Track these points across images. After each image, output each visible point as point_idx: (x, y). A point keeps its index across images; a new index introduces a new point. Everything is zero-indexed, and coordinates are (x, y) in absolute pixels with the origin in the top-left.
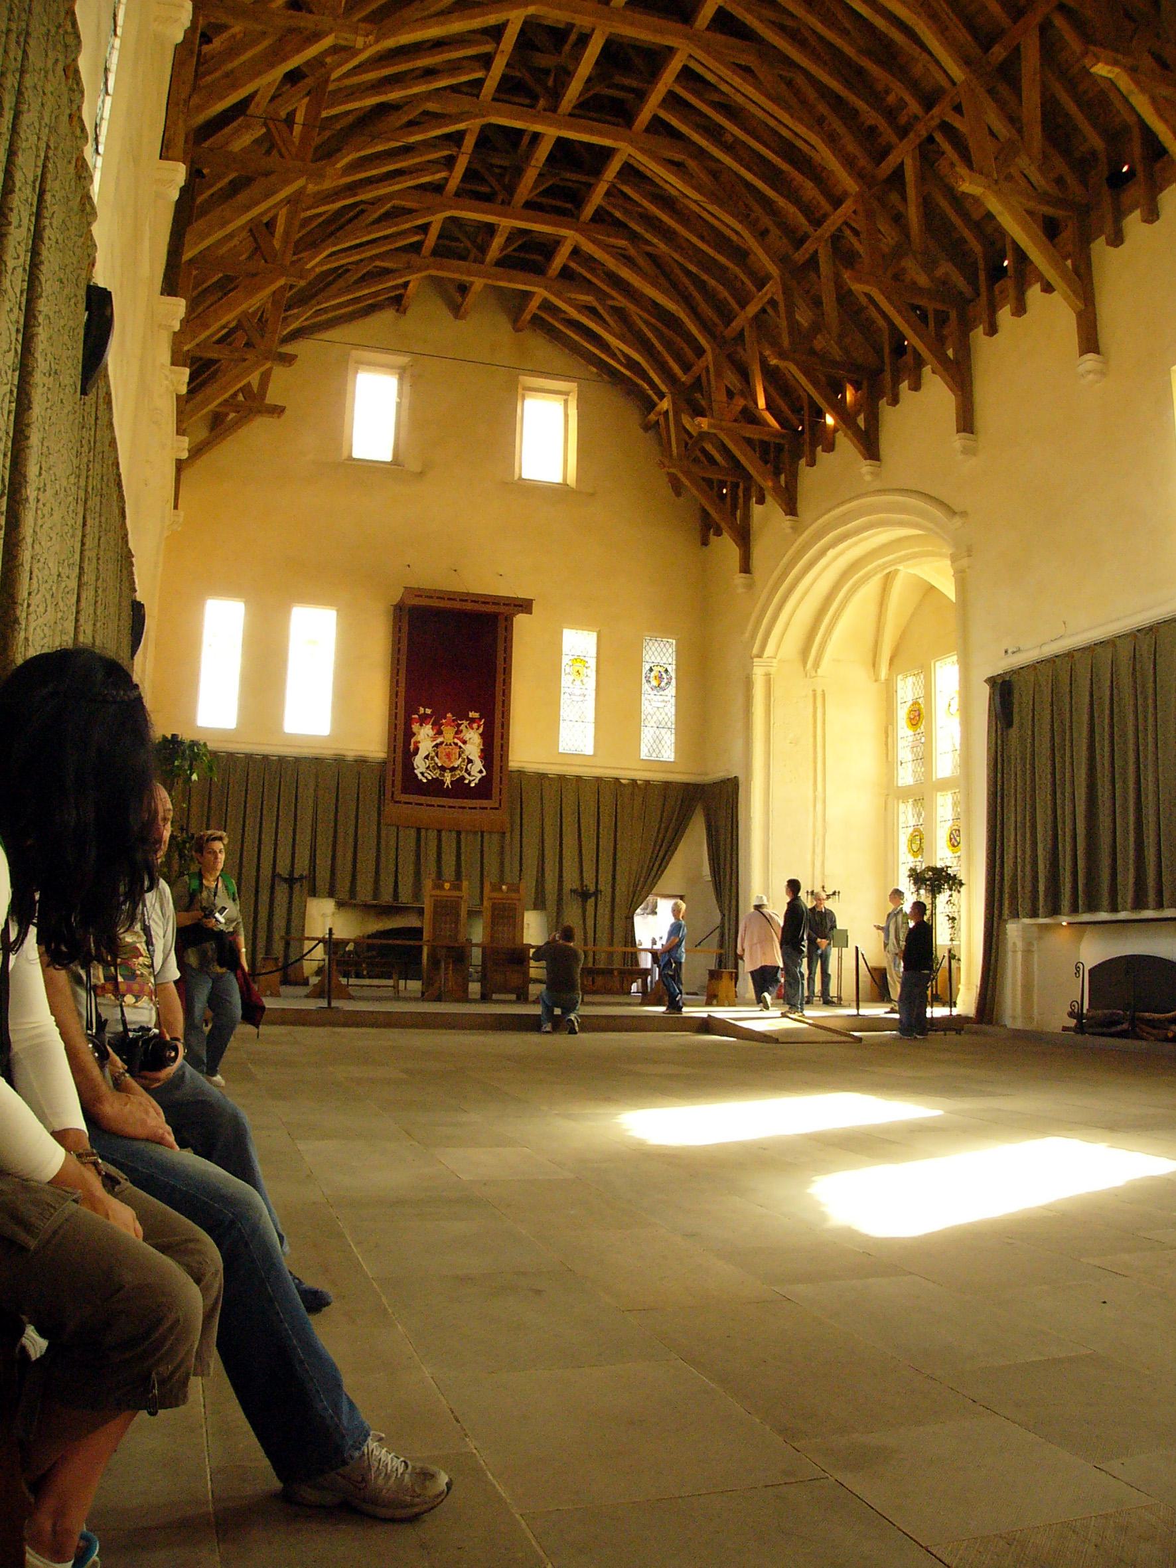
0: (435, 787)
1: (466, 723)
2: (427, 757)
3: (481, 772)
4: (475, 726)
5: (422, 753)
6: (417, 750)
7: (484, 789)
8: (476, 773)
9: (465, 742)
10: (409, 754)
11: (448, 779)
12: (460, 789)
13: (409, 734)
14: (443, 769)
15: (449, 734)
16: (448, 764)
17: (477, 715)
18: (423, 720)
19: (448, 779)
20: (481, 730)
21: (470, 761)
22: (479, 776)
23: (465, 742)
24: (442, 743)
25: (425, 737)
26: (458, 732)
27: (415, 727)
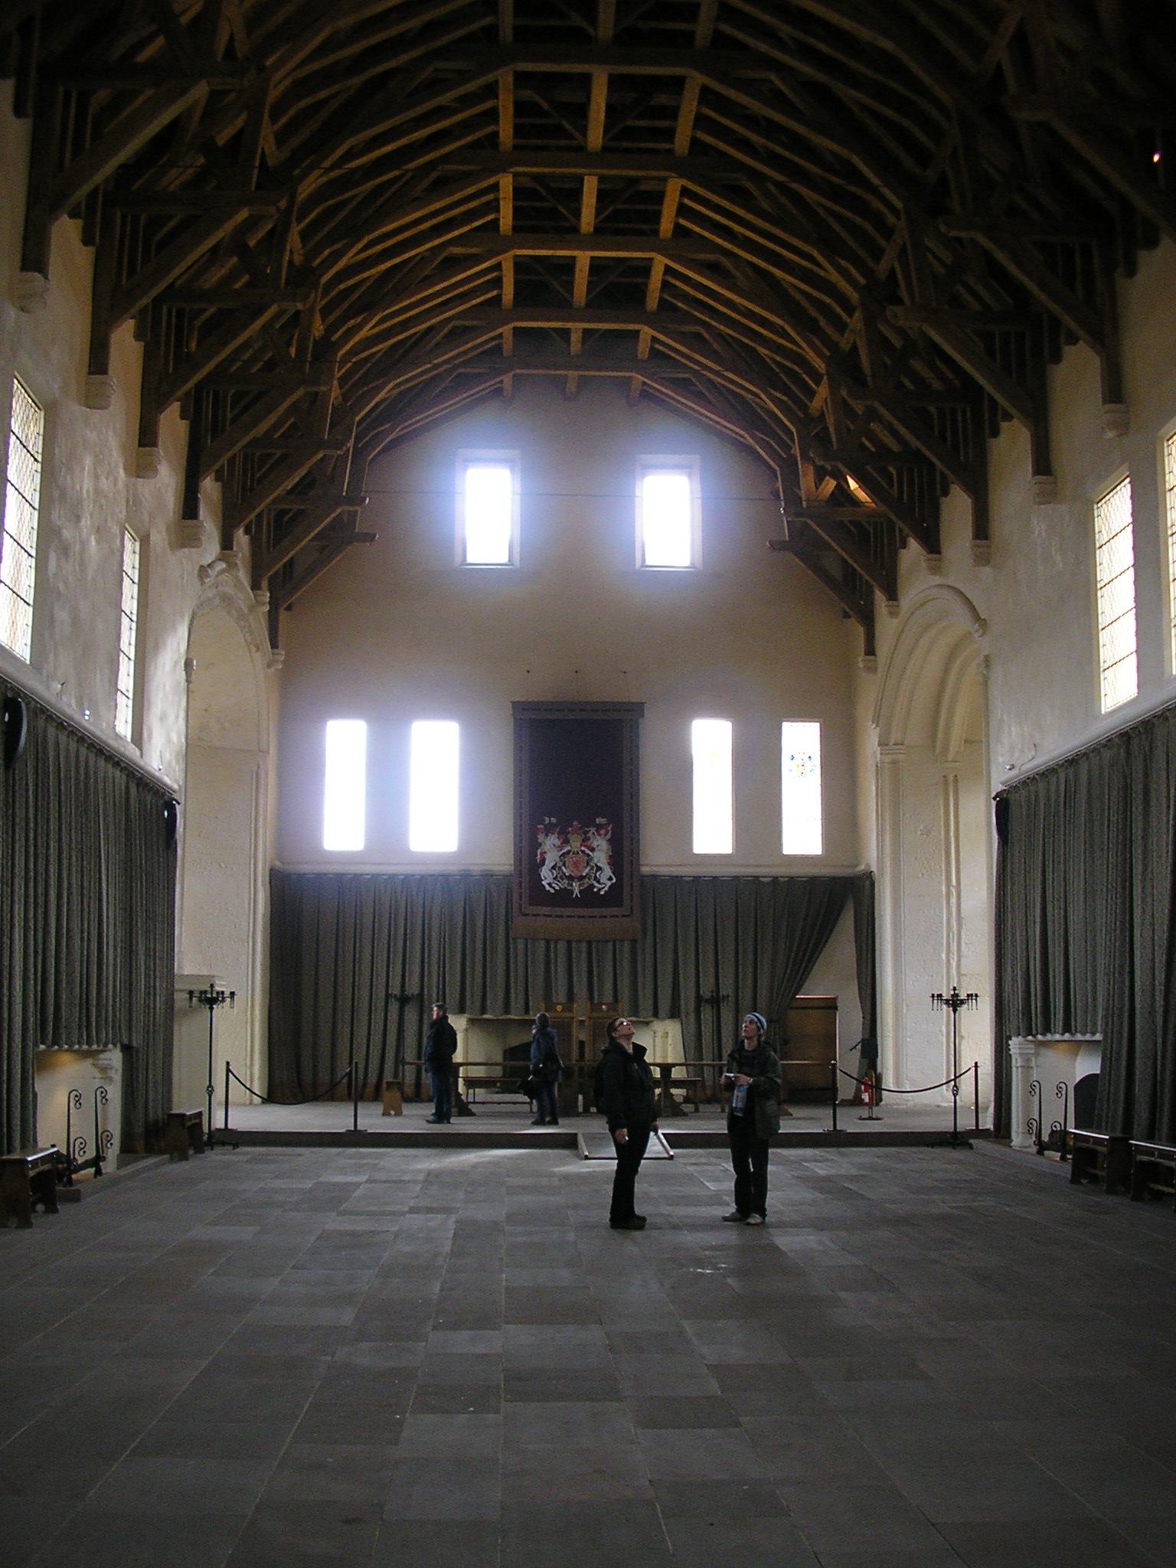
0: (562, 898)
1: (593, 830)
2: (553, 868)
3: (610, 879)
4: (602, 832)
5: (549, 863)
6: (543, 861)
7: (614, 896)
8: (606, 879)
9: (593, 850)
10: (535, 866)
11: (576, 888)
12: (590, 897)
13: (535, 845)
14: (571, 878)
15: (576, 843)
16: (576, 873)
17: (603, 821)
18: (548, 830)
19: (576, 888)
20: (609, 836)
21: (599, 869)
22: (609, 883)
23: (593, 850)
24: (569, 852)
25: (550, 847)
26: (586, 840)
27: (541, 837)
